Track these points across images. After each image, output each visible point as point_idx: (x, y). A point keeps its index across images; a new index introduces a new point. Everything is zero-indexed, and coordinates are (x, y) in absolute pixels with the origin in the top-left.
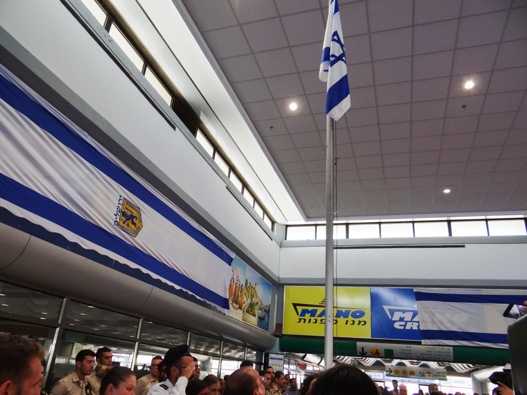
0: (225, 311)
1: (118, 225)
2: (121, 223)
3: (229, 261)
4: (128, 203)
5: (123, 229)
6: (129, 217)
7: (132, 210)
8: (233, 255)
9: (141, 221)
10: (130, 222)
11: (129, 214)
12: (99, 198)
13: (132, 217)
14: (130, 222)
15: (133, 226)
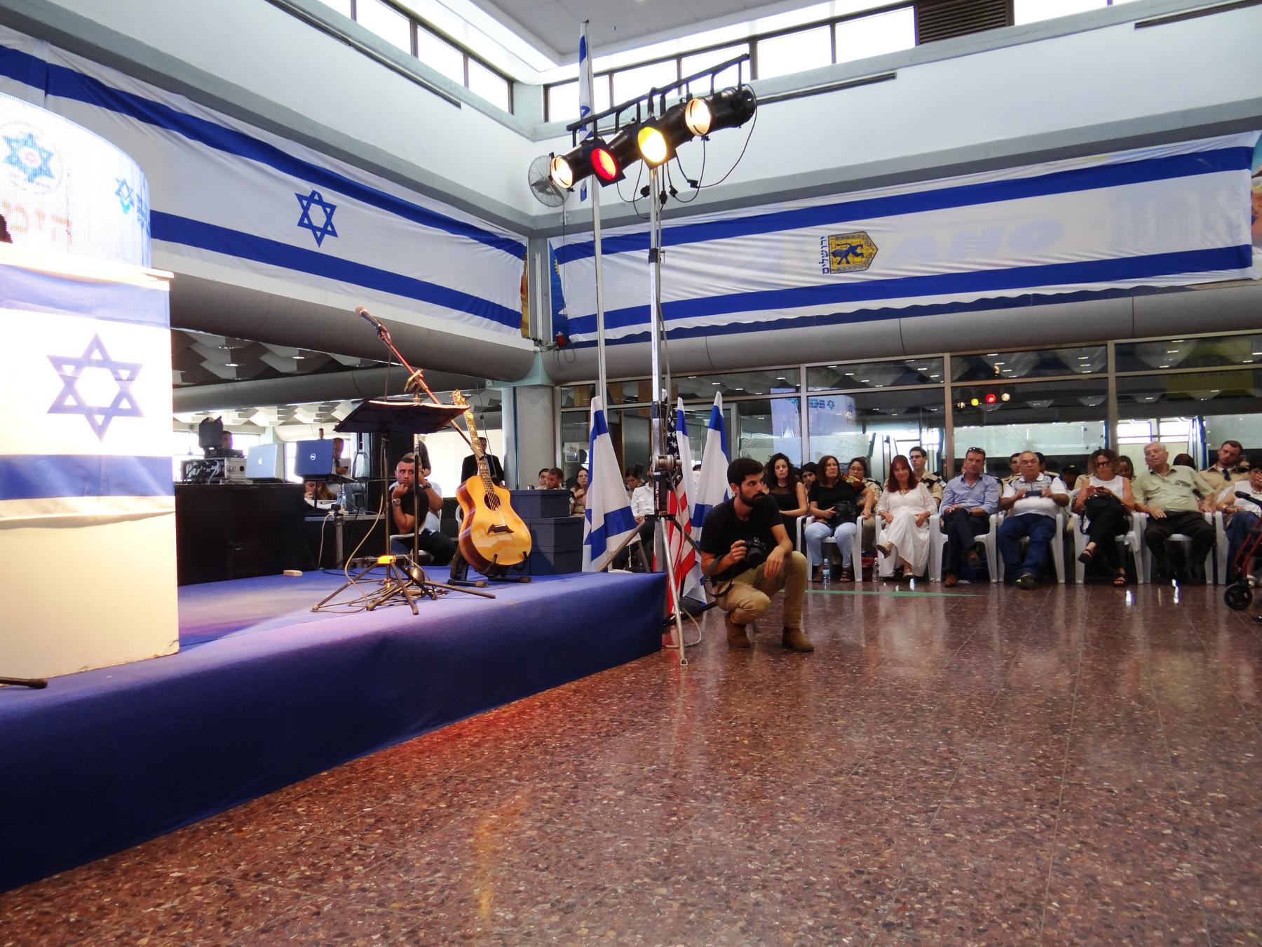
0: (1248, 272)
1: (829, 270)
2: (835, 266)
3: (1239, 159)
4: (837, 237)
5: (839, 271)
6: (845, 253)
7: (849, 241)
8: (1249, 140)
9: (871, 244)
10: (850, 258)
11: (845, 248)
12: (795, 258)
13: (852, 250)
14: (850, 258)
15: (858, 259)
